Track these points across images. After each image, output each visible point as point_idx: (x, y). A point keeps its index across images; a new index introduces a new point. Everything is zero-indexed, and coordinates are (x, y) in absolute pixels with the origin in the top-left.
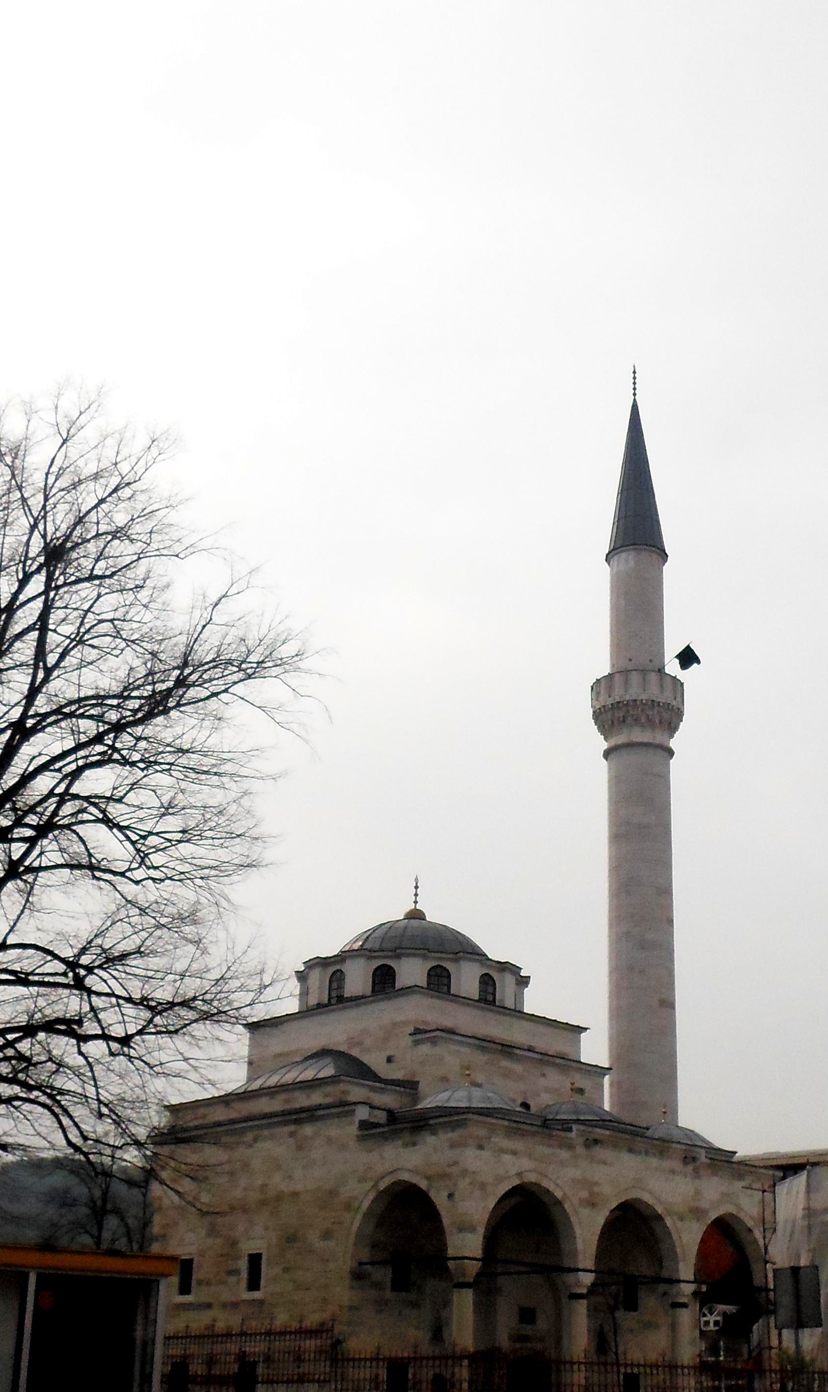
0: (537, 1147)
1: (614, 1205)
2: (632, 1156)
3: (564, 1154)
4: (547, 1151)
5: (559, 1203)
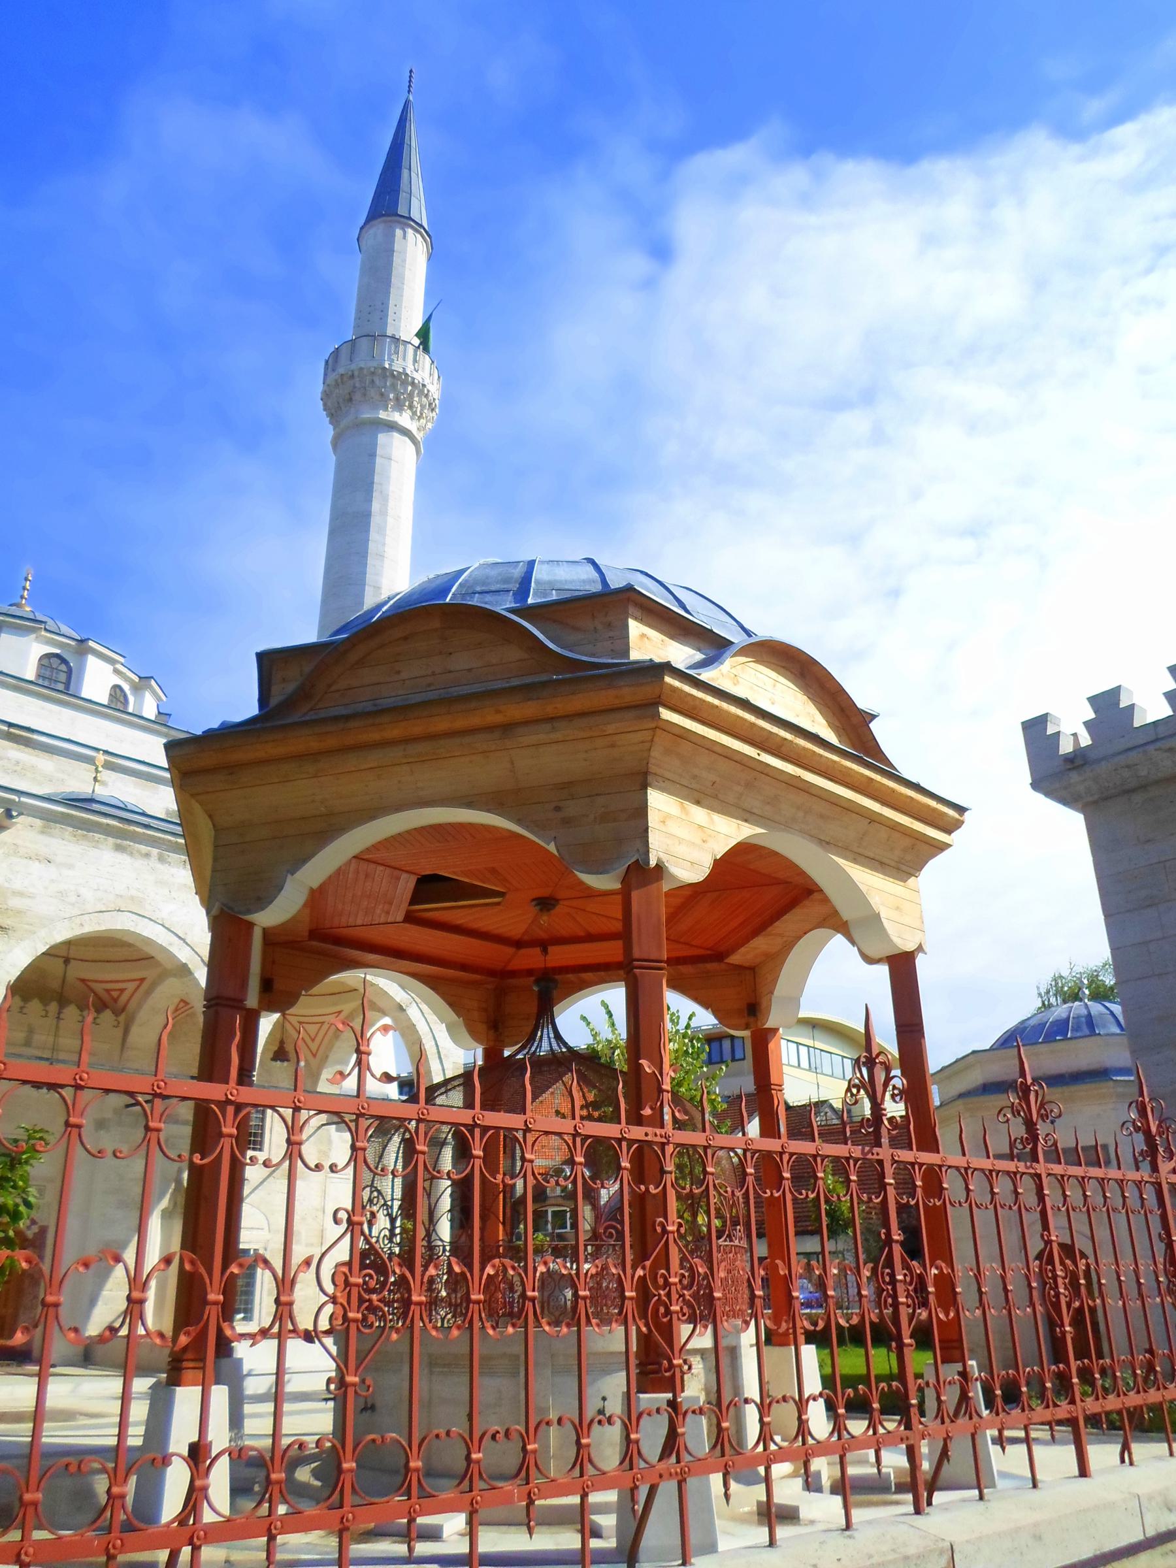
1: (62, 933)
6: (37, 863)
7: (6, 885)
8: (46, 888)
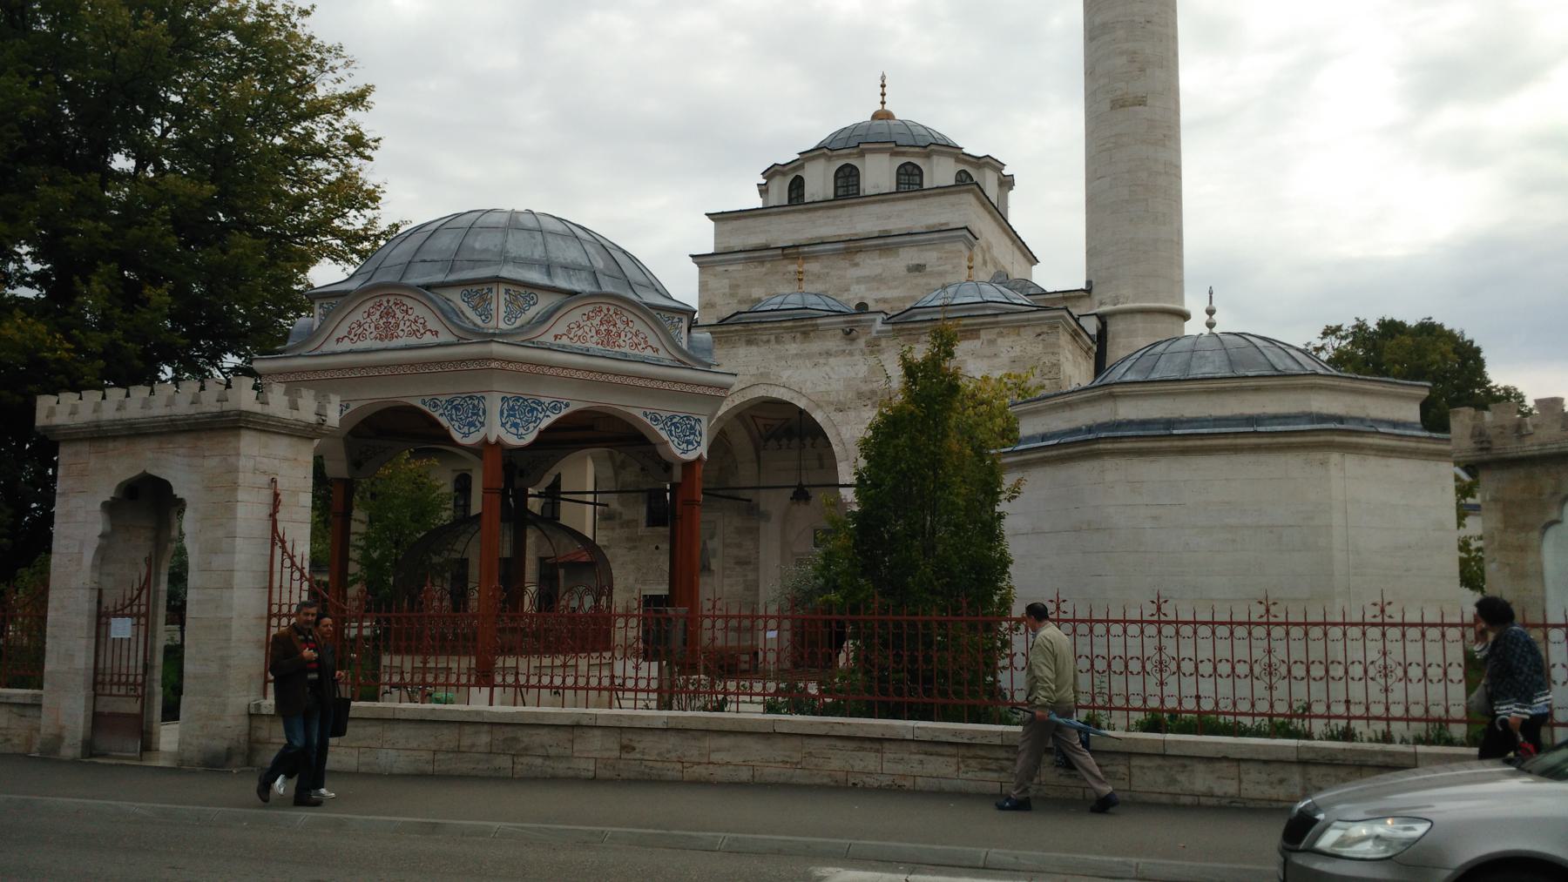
2: (754, 349)
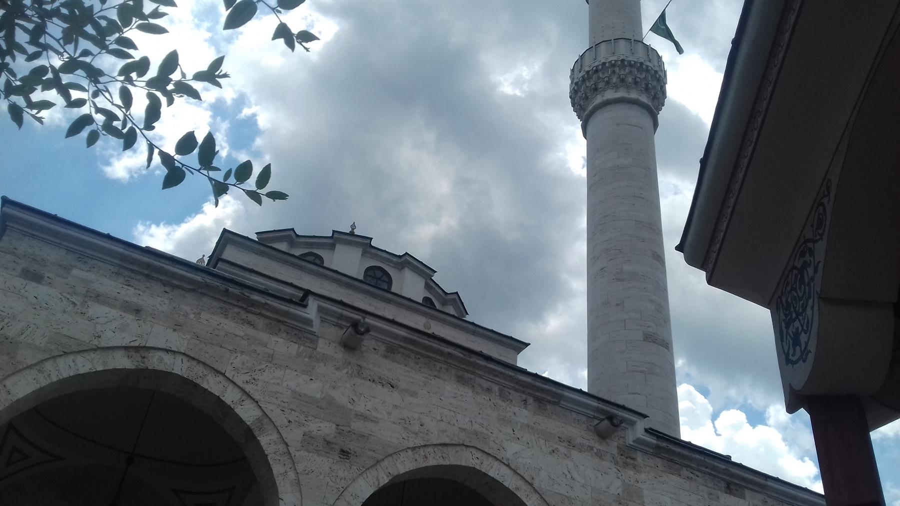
0: (204, 316)
3: (281, 345)
4: (229, 325)
5: (249, 434)
6: (380, 387)
7: (350, 406)
8: (389, 414)
